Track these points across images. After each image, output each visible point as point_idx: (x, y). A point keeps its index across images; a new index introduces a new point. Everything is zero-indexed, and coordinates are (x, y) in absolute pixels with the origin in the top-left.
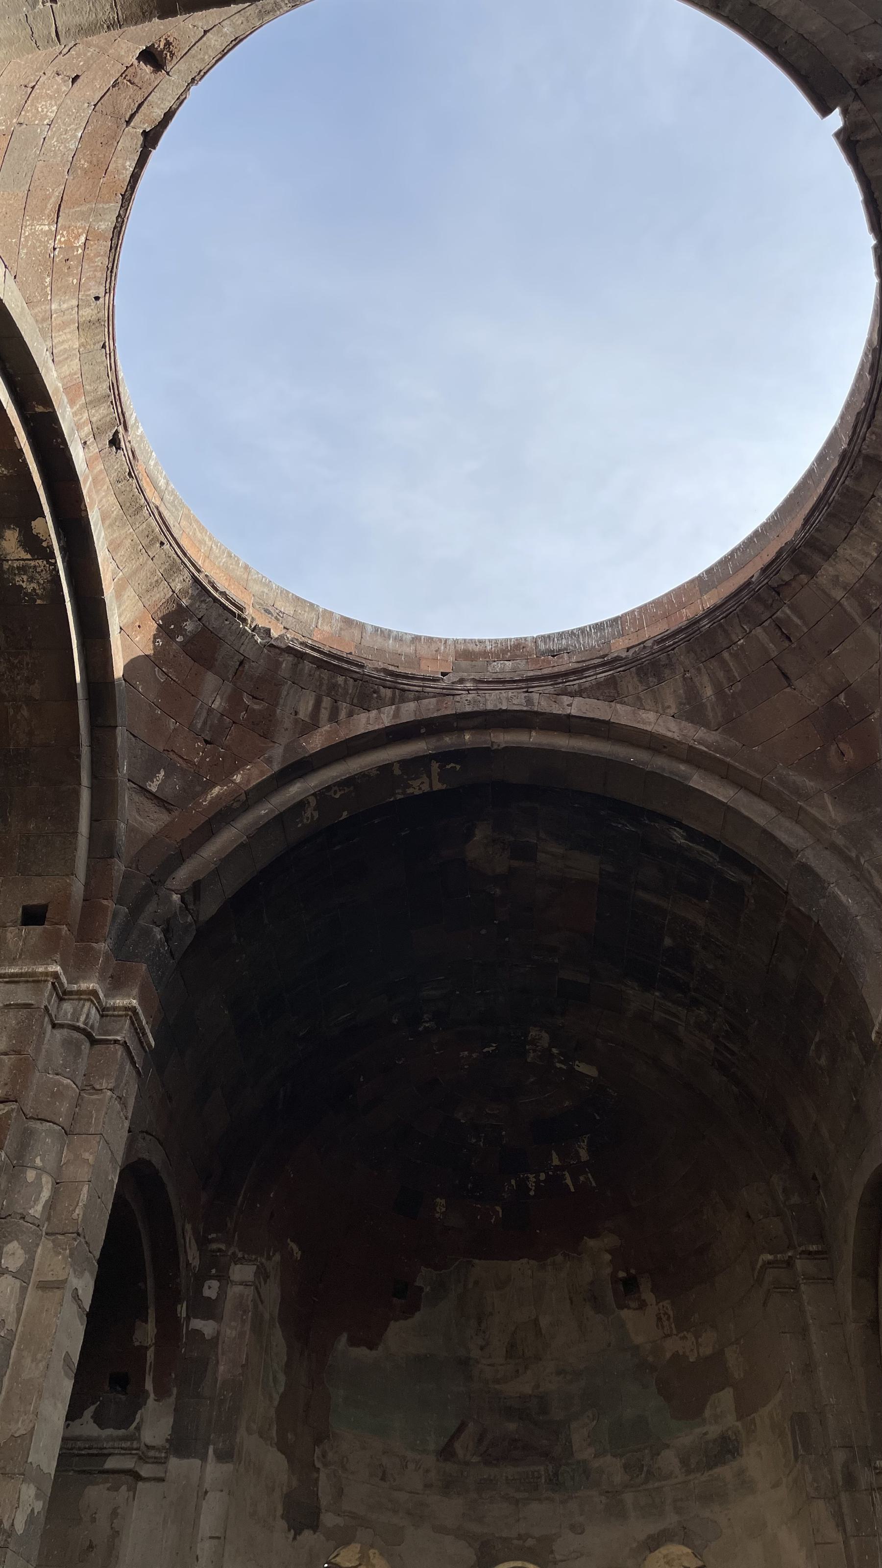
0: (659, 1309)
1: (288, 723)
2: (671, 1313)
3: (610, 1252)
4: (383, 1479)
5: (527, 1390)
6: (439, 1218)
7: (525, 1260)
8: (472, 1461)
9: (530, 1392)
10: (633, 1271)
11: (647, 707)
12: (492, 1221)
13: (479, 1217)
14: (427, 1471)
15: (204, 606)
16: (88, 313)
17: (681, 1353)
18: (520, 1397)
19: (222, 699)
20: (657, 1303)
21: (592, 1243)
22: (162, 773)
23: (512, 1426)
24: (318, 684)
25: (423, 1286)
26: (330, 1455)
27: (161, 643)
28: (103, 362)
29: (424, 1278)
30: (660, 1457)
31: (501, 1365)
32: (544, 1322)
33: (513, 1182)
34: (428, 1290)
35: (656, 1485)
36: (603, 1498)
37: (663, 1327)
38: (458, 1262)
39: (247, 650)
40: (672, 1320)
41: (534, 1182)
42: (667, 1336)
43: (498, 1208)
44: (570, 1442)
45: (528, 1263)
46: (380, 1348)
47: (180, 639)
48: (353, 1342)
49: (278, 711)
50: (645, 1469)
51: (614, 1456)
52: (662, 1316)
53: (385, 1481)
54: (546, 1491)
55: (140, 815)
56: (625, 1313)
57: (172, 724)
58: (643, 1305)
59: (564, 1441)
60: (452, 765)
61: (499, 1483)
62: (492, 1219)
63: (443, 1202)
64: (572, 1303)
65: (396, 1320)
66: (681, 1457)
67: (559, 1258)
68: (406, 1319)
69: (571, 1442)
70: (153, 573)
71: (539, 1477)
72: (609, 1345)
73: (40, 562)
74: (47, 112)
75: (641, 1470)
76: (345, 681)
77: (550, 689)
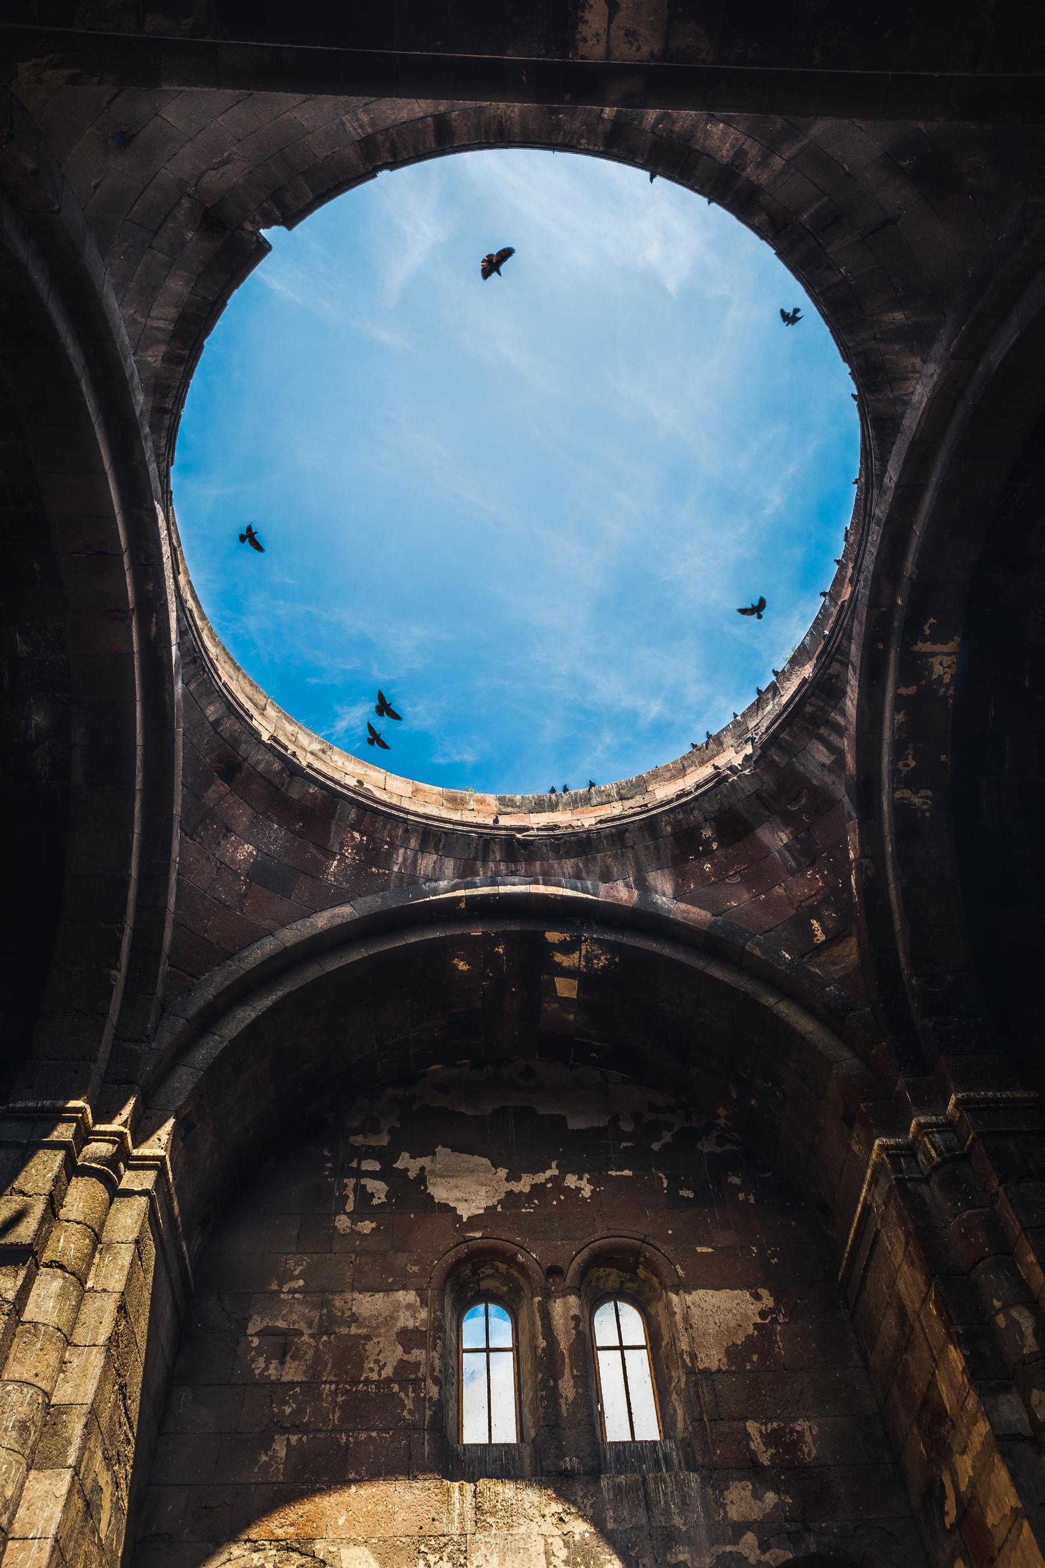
1: (829, 778)
11: (911, 389)
15: (695, 812)
16: (413, 843)
19: (782, 831)
22: (814, 922)
24: (805, 732)
27: (709, 865)
28: (457, 838)
39: (749, 788)
47: (715, 846)
49: (815, 782)
55: (838, 964)
57: (779, 890)
60: (926, 627)
70: (647, 848)
73: (583, 947)
74: (246, 852)
76: (811, 705)
77: (875, 491)
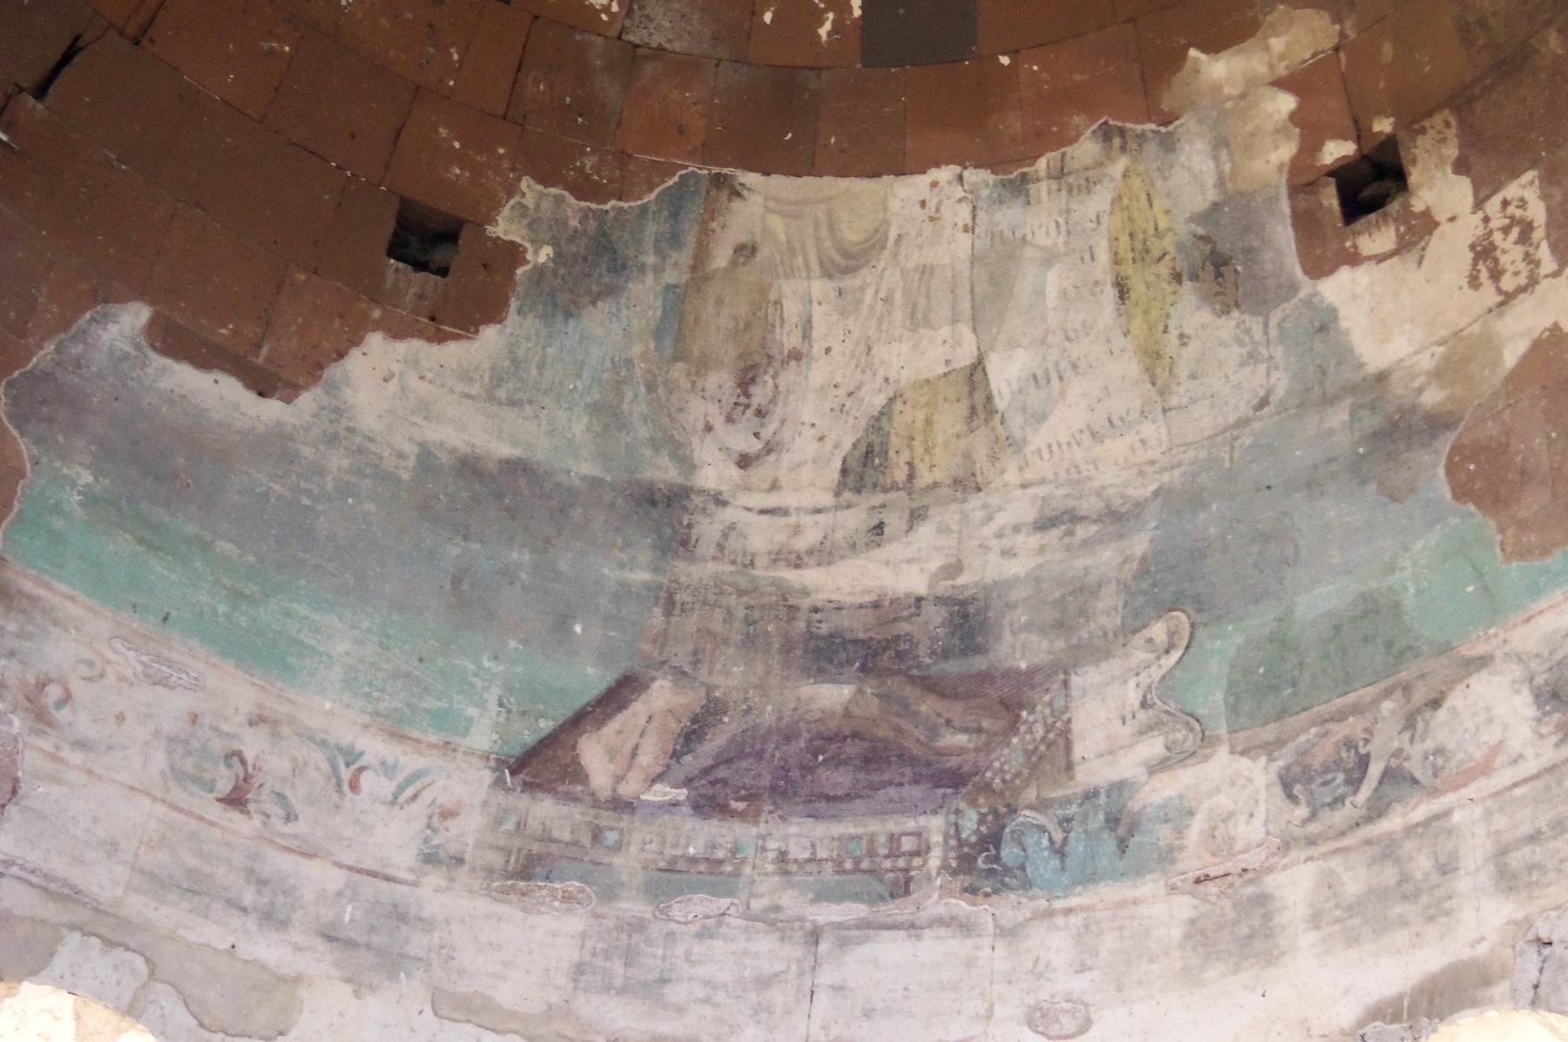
0: (1486, 220)
2: (1537, 212)
3: (1281, 84)
4: (236, 800)
5: (913, 582)
7: (945, 174)
8: (643, 797)
10: (1383, 126)
12: (823, 32)
13: (768, 17)
14: (447, 814)
18: (876, 605)
20: (1478, 205)
25: (527, 245)
30: (1442, 714)
32: (1005, 374)
34: (542, 259)
35: (1420, 813)
36: (1184, 907)
37: (1496, 275)
38: (676, 179)
40: (1538, 234)
42: (1508, 298)
44: (1066, 734)
45: (960, 178)
46: (308, 401)
50: (1375, 770)
52: (1497, 237)
54: (941, 898)
56: (1338, 288)
59: (1039, 731)
61: (748, 870)
62: (821, 23)
64: (1122, 290)
65: (398, 332)
66: (1539, 680)
67: (1086, 149)
68: (440, 338)
69: (1068, 731)
71: (922, 851)
72: (1264, 403)
75: (1355, 783)
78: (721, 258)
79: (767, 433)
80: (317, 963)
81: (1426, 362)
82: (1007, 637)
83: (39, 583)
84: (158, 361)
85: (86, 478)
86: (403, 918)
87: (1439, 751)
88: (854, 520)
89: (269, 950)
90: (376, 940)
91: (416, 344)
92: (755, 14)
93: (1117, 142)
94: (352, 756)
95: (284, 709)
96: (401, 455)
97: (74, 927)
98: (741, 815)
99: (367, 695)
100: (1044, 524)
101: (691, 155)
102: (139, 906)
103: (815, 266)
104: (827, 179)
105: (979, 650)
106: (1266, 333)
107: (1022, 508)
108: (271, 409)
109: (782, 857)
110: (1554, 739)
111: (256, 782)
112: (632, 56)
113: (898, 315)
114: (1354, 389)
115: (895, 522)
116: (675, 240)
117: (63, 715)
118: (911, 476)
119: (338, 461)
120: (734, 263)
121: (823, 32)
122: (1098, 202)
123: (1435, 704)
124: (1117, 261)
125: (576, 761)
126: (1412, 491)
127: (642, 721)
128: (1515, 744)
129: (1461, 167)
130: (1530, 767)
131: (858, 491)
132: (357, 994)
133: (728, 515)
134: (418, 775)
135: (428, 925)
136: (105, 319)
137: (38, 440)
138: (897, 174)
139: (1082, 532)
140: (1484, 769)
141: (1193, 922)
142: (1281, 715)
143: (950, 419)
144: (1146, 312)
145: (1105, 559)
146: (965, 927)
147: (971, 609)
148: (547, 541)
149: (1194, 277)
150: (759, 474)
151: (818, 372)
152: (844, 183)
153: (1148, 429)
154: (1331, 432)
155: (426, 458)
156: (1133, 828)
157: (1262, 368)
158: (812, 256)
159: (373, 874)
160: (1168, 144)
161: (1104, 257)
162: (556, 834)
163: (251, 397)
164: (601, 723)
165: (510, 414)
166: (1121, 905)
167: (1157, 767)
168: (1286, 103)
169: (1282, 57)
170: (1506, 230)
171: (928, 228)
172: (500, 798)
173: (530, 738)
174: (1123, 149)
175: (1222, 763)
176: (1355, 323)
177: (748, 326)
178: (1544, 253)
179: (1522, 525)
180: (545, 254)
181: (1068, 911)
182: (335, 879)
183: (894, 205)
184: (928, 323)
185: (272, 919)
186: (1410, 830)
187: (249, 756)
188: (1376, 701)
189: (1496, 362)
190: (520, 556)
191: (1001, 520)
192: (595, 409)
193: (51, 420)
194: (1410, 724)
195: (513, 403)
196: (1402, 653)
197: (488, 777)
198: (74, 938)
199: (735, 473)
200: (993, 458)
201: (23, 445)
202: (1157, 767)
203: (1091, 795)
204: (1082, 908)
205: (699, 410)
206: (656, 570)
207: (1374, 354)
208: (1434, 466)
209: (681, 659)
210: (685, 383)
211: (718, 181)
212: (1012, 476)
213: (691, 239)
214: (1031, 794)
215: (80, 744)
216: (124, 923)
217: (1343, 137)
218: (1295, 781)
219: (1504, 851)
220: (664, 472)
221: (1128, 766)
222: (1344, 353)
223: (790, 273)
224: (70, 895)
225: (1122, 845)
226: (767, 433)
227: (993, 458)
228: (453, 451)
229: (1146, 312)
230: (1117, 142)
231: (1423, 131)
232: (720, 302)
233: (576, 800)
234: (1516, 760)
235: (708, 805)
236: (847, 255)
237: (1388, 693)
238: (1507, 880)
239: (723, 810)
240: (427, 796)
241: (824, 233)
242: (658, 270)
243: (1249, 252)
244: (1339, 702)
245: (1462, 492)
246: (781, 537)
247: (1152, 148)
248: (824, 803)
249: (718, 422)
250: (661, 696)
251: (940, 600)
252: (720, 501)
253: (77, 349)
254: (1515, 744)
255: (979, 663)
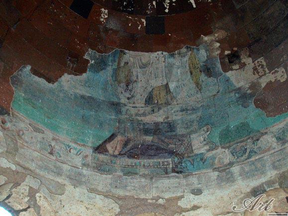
0: (255, 64)
2: (264, 63)
3: (217, 41)
4: (51, 153)
5: (160, 120)
6: (103, 21)
7: (160, 53)
9: (162, 121)
10: (235, 49)
12: (139, 28)
13: (130, 25)
14: (86, 156)
17: (273, 81)
20: (253, 62)
21: (206, 38)
23: (149, 138)
26: (8, 125)
29: (89, 55)
30: (259, 141)
31: (142, 107)
32: (172, 86)
33: (154, 3)
35: (257, 158)
36: (216, 173)
37: (258, 73)
41: (168, 3)
42: (261, 77)
43: (143, 20)
44: (191, 145)
46: (55, 84)
48: (35, 72)
50: (248, 151)
51: (224, 148)
52: (257, 67)
53: (53, 155)
56: (229, 74)
58: (243, 66)
63: (106, 11)
64: (191, 73)
65: (69, 74)
67: (184, 50)
68: (76, 75)
71: (169, 164)
72: (218, 92)
78: (122, 65)
79: (132, 94)
80: (67, 182)
81: (247, 86)
82: (178, 129)
83: (18, 113)
84: (33, 75)
85: (23, 95)
86: (80, 175)
87: (260, 147)
88: (149, 109)
89: (60, 180)
90: (77, 179)
91: (72, 76)
92: (128, 24)
93: (189, 49)
94: (69, 146)
95: (57, 137)
96: (71, 95)
97: (28, 174)
98: (136, 158)
99: (70, 136)
100: (182, 110)
101: (117, 47)
102: (38, 171)
103: (138, 67)
104: (140, 53)
105: (174, 131)
106: (217, 81)
107: (177, 108)
108: (51, 85)
109: (144, 166)
110: (280, 145)
111: (54, 150)
112: (106, 30)
113: (153, 75)
114: (235, 90)
115: (156, 110)
116: (115, 61)
117: (23, 137)
118: (157, 102)
119: (61, 95)
120: (124, 65)
121: (139, 28)
122: (186, 59)
123: (258, 140)
124: (190, 68)
125: (106, 148)
126: (248, 106)
127: (116, 142)
128: (274, 146)
129: (250, 56)
130: (277, 150)
131: (149, 104)
132: (74, 188)
133: (127, 107)
134: (80, 150)
135: (84, 176)
136: (24, 67)
137: (16, 88)
138: (152, 52)
139: (188, 112)
140: (269, 150)
141: (218, 176)
142: (230, 142)
143: (163, 93)
144: (196, 77)
145: (194, 117)
146: (178, 177)
147: (171, 124)
148: (97, 111)
149: (204, 72)
150: (131, 101)
151: (139, 85)
152: (142, 53)
153: (199, 95)
154: (232, 97)
155: (76, 97)
156: (205, 160)
157: (217, 86)
158: (138, 64)
159: (75, 167)
160: (198, 50)
161: (188, 68)
162: (105, 161)
163: (47, 83)
164: (110, 142)
165: (88, 89)
166: (205, 173)
167: (208, 151)
168: (218, 44)
169: (217, 37)
170: (259, 66)
171: (157, 61)
172: (94, 154)
173: (98, 144)
174: (190, 50)
175: (220, 150)
176: (233, 80)
177: (127, 76)
178: (266, 69)
179: (269, 112)
180: (93, 62)
181: (196, 174)
182: (69, 168)
183: (151, 57)
184: (158, 77)
185: (59, 174)
186: (256, 160)
187: (53, 145)
188: (247, 140)
189: (261, 87)
190: (92, 113)
191: (174, 110)
192: (103, 89)
193: (17, 84)
194: (254, 143)
195: (89, 87)
196: (250, 132)
197: (91, 151)
198: (29, 176)
199: (127, 100)
200: (172, 99)
201: (14, 88)
202: (208, 151)
203: (198, 155)
204: (198, 174)
205: (120, 89)
206: (115, 116)
207: (238, 85)
208: (252, 102)
209: (122, 131)
210: (117, 85)
211: (121, 51)
212: (175, 103)
213: (117, 61)
214: (186, 155)
215: (27, 142)
216: (36, 174)
217: (227, 50)
218: (234, 153)
219: (274, 163)
220: (116, 100)
221: (203, 151)
222: (232, 85)
223: (134, 67)
224: (25, 168)
225: (204, 163)
226: (132, 94)
227: (172, 99)
228: (80, 94)
229: (196, 77)
230: (189, 49)
231: (242, 50)
232: (122, 71)
233: (107, 155)
234: (274, 148)
235: (131, 156)
236: (143, 64)
237: (249, 138)
238: (275, 168)
239: (133, 157)
240: (82, 154)
241: (140, 61)
242: (112, 66)
243: (213, 68)
244: (239, 140)
245: (257, 106)
246: (136, 112)
247: (195, 50)
248: (150, 156)
249: (123, 92)
250: (119, 138)
251: (165, 123)
252: (125, 105)
253: (20, 72)
254: (274, 146)
255: (174, 133)
